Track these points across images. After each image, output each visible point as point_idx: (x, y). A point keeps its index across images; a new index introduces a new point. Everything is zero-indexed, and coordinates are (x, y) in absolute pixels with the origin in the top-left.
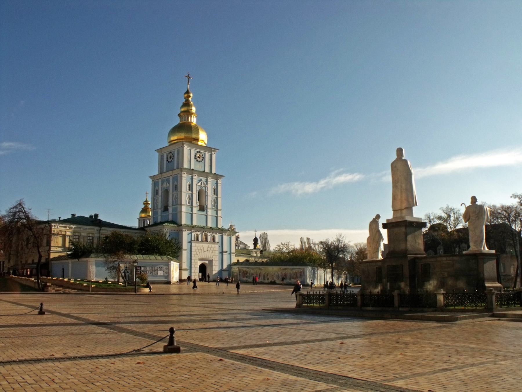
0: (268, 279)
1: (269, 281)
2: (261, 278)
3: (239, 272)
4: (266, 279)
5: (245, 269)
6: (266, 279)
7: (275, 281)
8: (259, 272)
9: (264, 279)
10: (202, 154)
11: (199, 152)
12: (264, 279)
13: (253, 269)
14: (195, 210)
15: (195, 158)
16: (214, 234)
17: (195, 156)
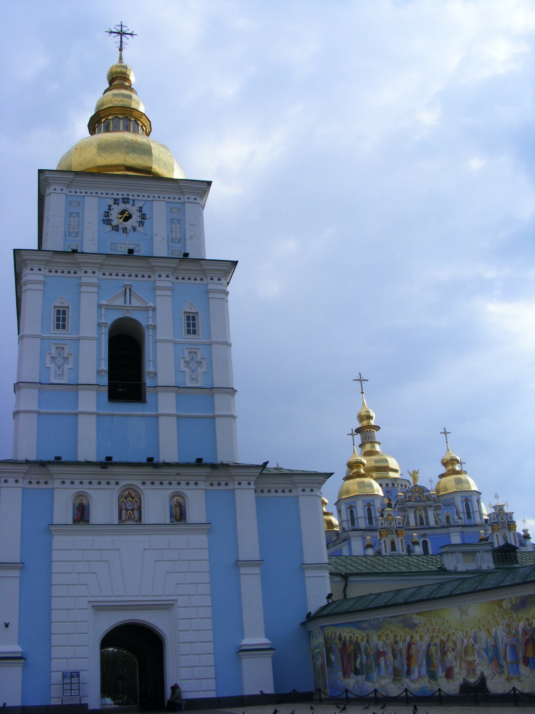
0: (449, 673)
1: (451, 687)
2: (415, 670)
3: (329, 650)
4: (441, 673)
5: (347, 633)
6: (441, 673)
7: (483, 680)
8: (404, 636)
9: (432, 676)
10: (138, 204)
11: (126, 201)
12: (432, 676)
13: (378, 627)
14: (90, 401)
15: (107, 221)
16: (183, 488)
17: (107, 214)
